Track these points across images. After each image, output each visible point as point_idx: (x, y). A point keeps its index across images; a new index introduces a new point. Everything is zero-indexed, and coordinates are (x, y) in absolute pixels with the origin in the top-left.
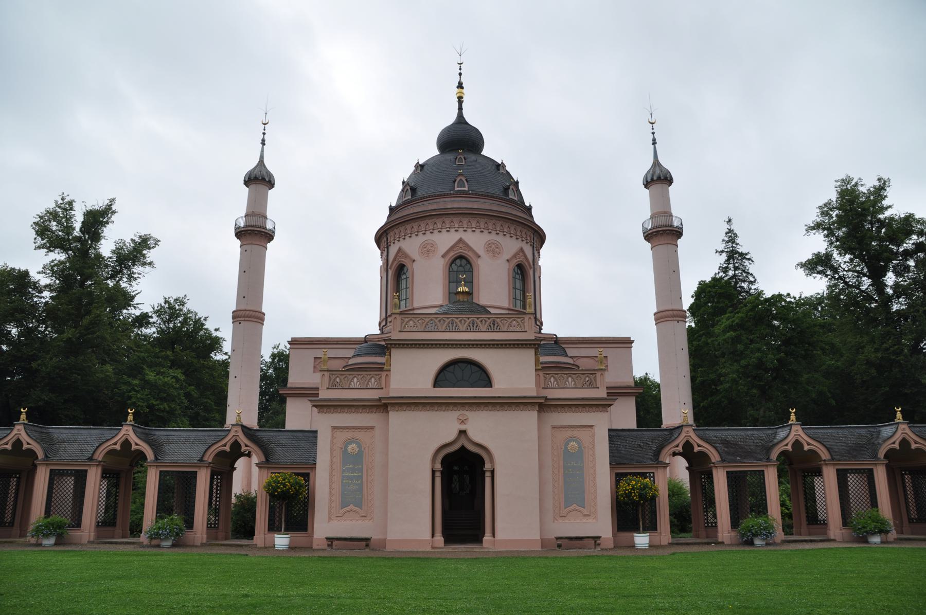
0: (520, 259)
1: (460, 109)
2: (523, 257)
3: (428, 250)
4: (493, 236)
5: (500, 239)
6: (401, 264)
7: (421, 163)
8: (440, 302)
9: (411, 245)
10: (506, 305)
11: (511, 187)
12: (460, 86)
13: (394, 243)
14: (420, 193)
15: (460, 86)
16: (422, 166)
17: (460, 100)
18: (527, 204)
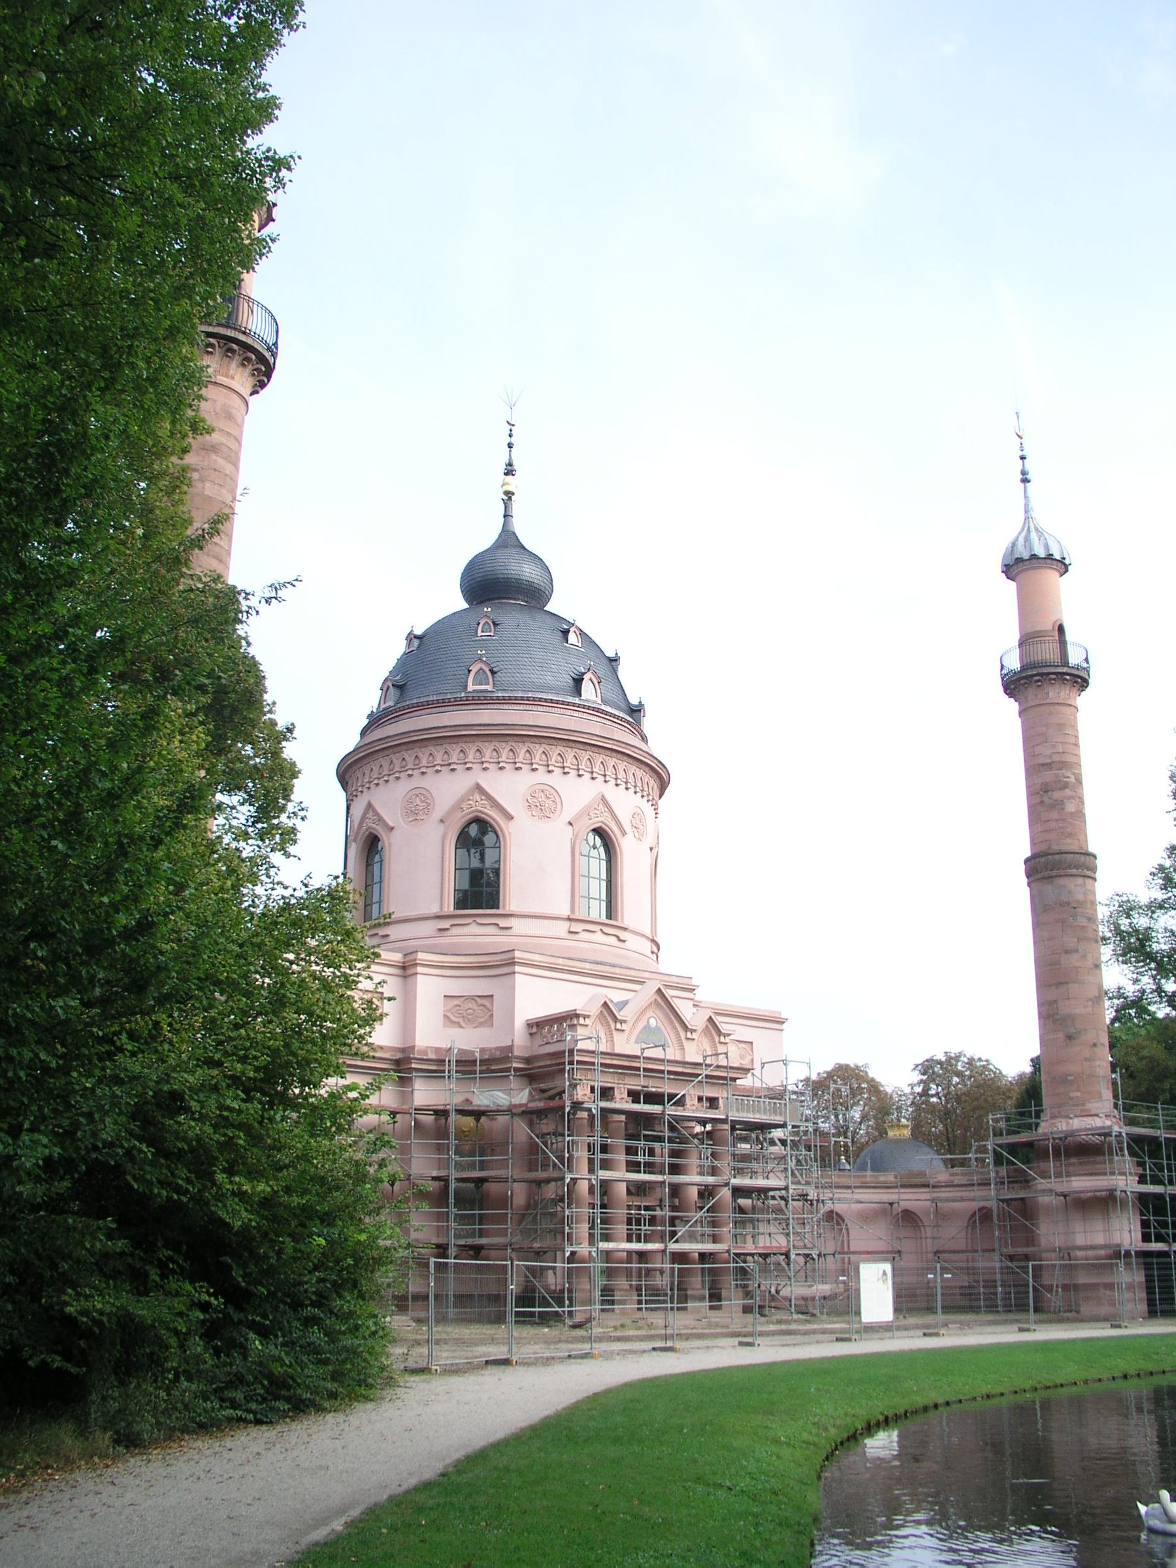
0: (601, 818)
2: (606, 814)
3: (417, 809)
4: (541, 776)
5: (556, 779)
6: (371, 833)
7: (419, 631)
8: (435, 909)
11: (586, 677)
12: (509, 471)
13: (362, 792)
15: (509, 471)
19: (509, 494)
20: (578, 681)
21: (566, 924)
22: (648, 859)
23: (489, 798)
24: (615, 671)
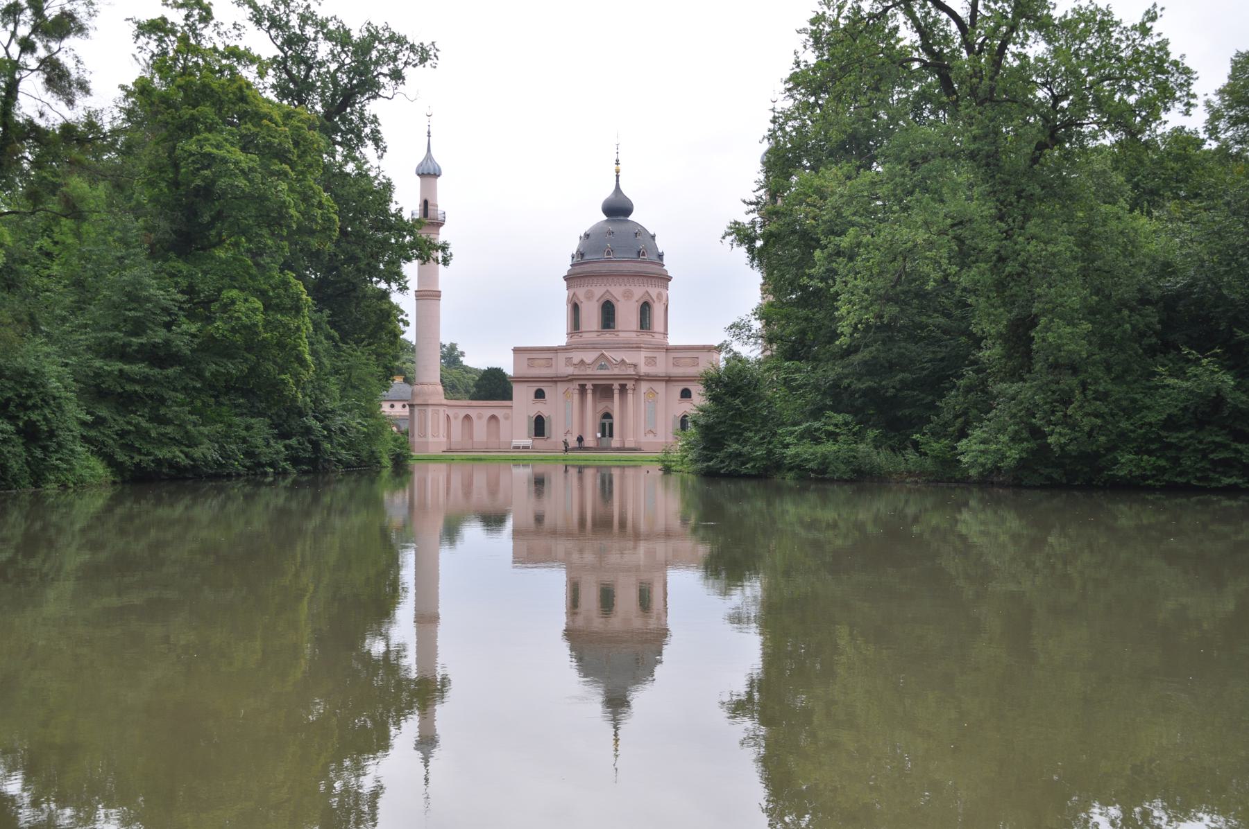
1: (617, 181)
3: (589, 296)
4: (628, 287)
5: (633, 288)
8: (596, 329)
9: (581, 292)
10: (635, 329)
12: (617, 163)
14: (587, 257)
15: (617, 163)
16: (588, 235)
17: (618, 176)
18: (660, 251)
19: (618, 172)
20: (639, 252)
21: (634, 335)
22: (663, 308)
23: (611, 294)
24: (654, 240)
